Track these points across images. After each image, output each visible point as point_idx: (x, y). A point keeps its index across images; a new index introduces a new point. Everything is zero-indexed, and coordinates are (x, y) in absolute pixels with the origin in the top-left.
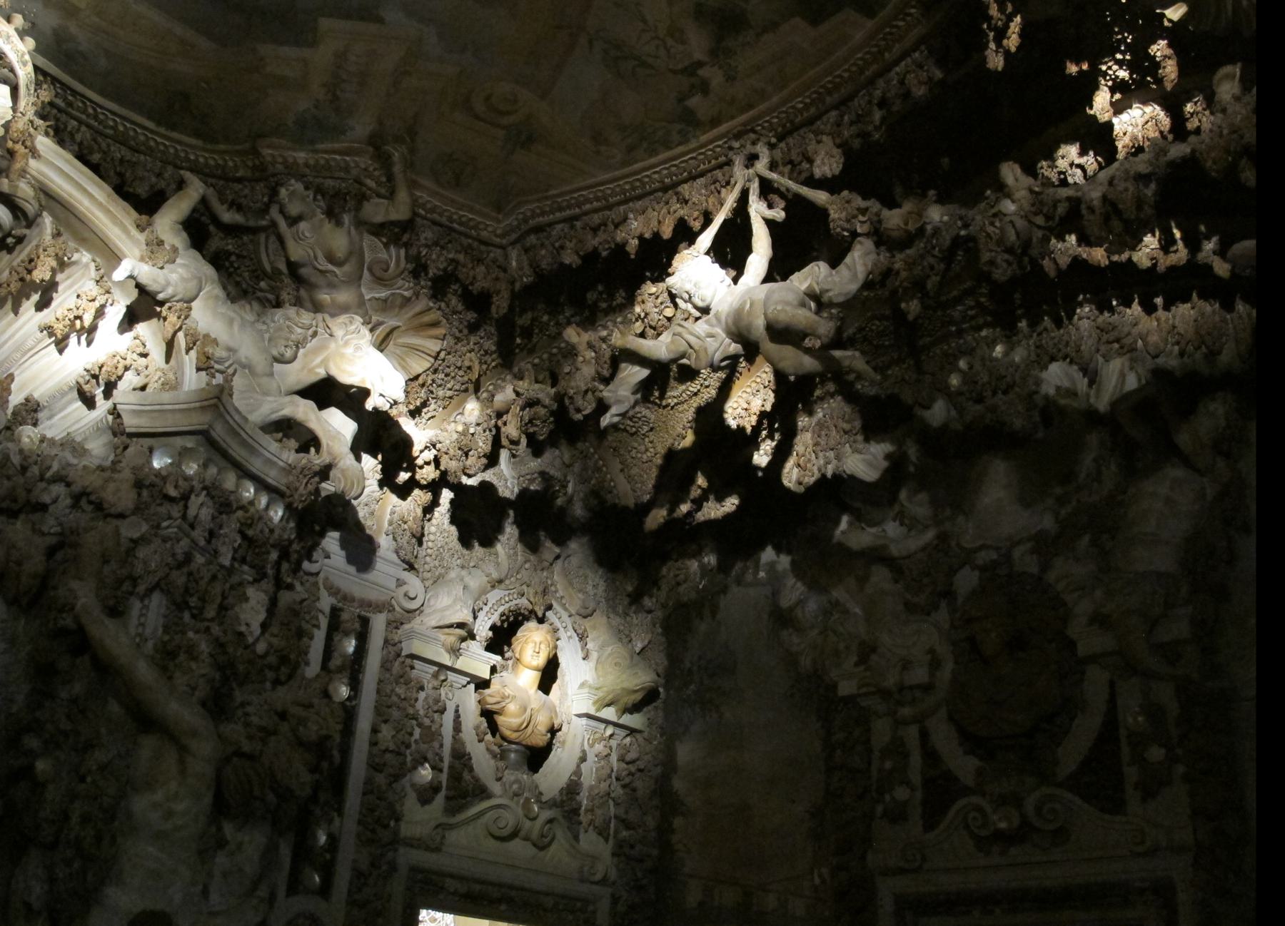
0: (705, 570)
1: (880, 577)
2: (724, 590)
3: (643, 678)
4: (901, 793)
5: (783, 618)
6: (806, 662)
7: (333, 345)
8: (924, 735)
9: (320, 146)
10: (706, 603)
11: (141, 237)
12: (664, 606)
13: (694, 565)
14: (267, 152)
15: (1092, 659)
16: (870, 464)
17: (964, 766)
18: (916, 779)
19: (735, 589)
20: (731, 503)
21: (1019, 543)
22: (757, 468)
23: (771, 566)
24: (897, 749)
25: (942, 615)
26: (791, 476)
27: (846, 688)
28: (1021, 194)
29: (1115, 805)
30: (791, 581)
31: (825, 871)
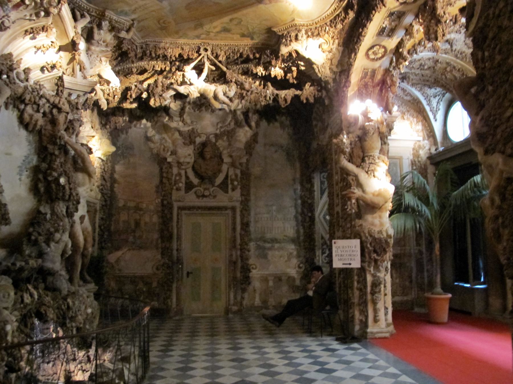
0: (124, 121)
1: (177, 135)
2: (131, 128)
3: (113, 149)
4: (181, 185)
5: (148, 139)
6: (155, 151)
7: (102, 66)
8: (186, 172)
9: (120, 17)
10: (124, 130)
11: (74, 30)
12: (110, 127)
13: (121, 119)
14: (107, 14)
15: (226, 163)
16: (175, 106)
17: (195, 181)
18: (184, 182)
19: (133, 129)
20: (135, 105)
21: (211, 134)
22: (142, 98)
23: (145, 125)
24: (179, 174)
25: (192, 147)
26: (152, 103)
27: (169, 160)
28: (271, 90)
29: (227, 192)
30: (151, 130)
31: (160, 200)
